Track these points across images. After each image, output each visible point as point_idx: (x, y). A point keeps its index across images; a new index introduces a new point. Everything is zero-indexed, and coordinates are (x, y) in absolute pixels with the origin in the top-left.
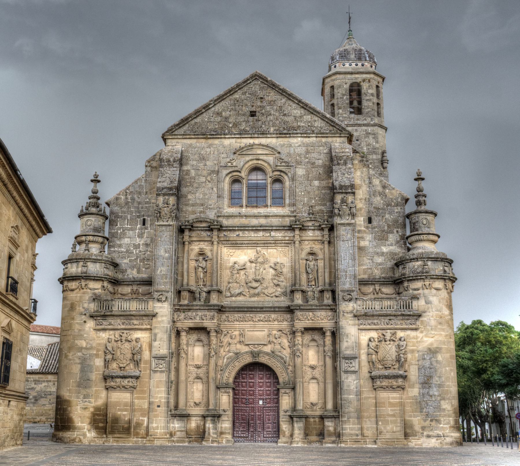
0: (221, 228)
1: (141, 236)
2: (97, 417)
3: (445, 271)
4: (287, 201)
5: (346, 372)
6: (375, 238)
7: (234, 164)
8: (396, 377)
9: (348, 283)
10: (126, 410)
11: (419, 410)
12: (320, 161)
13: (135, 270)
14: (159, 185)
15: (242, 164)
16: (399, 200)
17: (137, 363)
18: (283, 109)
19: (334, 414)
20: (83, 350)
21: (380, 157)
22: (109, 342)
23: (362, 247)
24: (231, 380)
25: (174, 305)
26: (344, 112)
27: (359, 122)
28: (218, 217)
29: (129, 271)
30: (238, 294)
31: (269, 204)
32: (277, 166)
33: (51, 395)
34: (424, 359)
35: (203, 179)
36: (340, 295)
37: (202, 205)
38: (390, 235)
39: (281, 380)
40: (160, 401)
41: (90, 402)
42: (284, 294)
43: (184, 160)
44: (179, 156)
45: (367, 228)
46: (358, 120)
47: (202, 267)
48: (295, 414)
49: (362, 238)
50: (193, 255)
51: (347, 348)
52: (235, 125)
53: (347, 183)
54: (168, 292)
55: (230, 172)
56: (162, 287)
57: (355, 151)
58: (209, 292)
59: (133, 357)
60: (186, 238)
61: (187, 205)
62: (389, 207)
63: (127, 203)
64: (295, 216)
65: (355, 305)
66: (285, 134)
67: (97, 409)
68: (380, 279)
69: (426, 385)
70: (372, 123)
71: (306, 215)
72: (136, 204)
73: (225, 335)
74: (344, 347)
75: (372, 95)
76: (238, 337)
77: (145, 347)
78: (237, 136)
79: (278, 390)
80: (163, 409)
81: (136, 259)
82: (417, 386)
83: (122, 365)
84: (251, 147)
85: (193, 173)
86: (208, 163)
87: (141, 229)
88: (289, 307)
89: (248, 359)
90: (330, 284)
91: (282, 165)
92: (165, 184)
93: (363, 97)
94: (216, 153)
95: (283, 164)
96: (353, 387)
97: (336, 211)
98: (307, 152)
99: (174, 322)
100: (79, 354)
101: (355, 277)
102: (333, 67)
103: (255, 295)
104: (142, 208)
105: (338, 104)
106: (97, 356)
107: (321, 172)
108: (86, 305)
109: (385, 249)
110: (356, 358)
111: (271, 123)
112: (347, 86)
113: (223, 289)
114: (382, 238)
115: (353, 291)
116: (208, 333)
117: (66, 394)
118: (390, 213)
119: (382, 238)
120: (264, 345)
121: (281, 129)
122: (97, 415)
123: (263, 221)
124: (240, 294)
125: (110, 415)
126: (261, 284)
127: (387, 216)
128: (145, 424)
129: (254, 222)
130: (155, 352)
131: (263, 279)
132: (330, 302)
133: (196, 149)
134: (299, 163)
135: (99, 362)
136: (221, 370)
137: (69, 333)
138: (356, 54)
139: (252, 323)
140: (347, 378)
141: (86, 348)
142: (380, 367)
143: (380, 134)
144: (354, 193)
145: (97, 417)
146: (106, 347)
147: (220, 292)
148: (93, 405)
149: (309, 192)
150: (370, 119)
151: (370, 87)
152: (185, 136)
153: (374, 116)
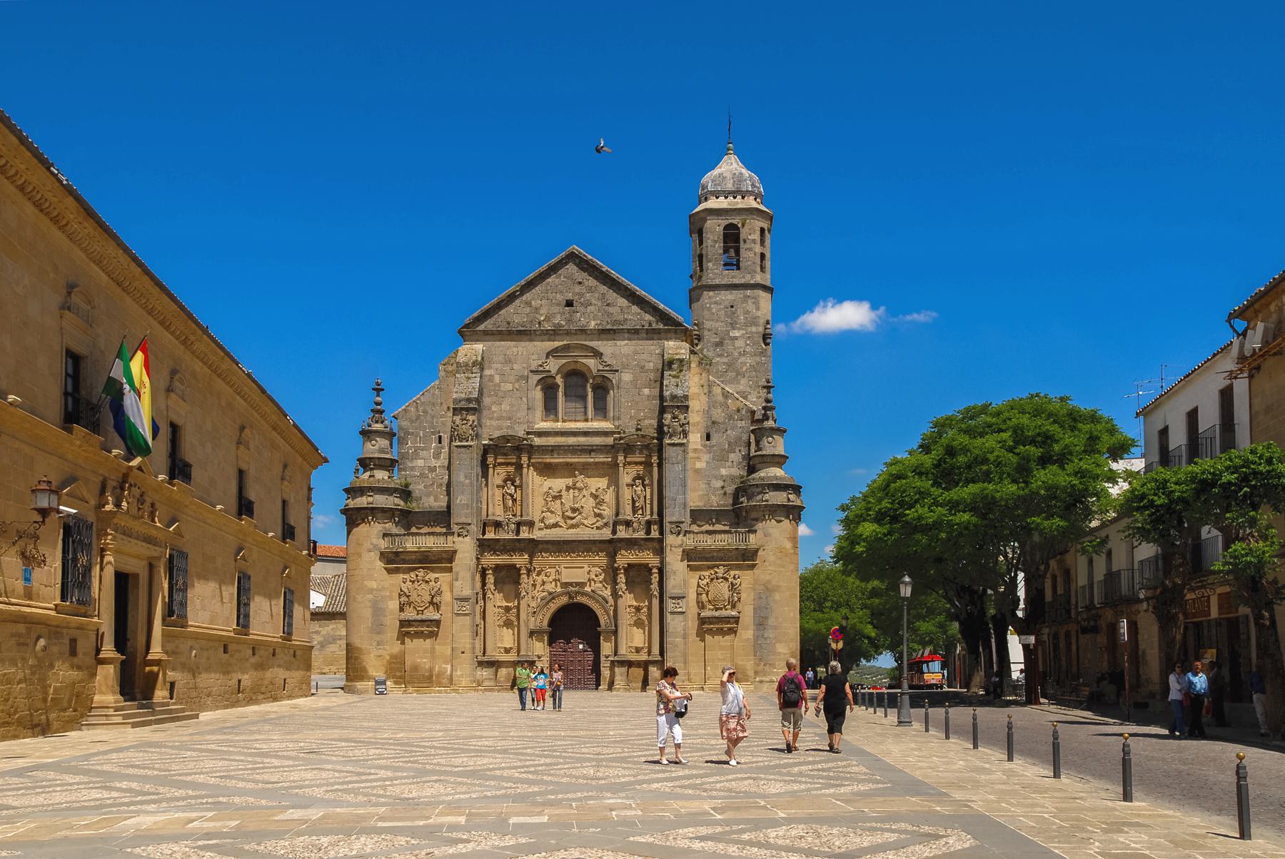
0: (531, 450)
1: (437, 456)
2: (393, 665)
3: (789, 499)
4: (612, 415)
5: (673, 613)
6: (714, 459)
7: (547, 368)
8: (727, 619)
9: (677, 513)
10: (426, 658)
11: (752, 653)
12: (651, 364)
13: (432, 497)
14: (455, 396)
15: (557, 367)
16: (744, 413)
17: (437, 607)
18: (607, 297)
19: (659, 658)
20: (374, 592)
21: (761, 329)
22: (404, 583)
23: (698, 469)
24: (546, 623)
25: (478, 540)
26: (715, 267)
27: (736, 281)
28: (528, 433)
29: (424, 499)
30: (553, 524)
31: (590, 417)
32: (598, 371)
33: (340, 639)
34: (760, 598)
35: (509, 387)
36: (667, 527)
37: (510, 419)
38: (732, 456)
39: (602, 622)
40: (465, 647)
41: (384, 649)
42: (606, 524)
43: (486, 365)
44: (480, 359)
45: (705, 446)
46: (733, 277)
47: (510, 495)
48: (616, 658)
49: (698, 458)
50: (499, 481)
51: (674, 587)
52: (548, 319)
53: (679, 392)
54: (470, 524)
55: (543, 378)
56: (463, 520)
57: (692, 352)
58: (519, 524)
59: (432, 598)
60: (490, 460)
61: (491, 419)
62: (731, 422)
63: (418, 417)
64: (619, 433)
65: (684, 538)
66: (609, 330)
67: (393, 657)
68: (718, 506)
69: (761, 627)
70: (752, 282)
71: (633, 431)
72: (429, 418)
73: (538, 574)
74: (671, 585)
75: (754, 241)
76: (553, 573)
77: (445, 588)
78: (551, 332)
79: (599, 634)
80: (468, 655)
81: (433, 484)
82: (752, 627)
83: (420, 609)
84: (566, 348)
85: (497, 379)
86: (515, 366)
87: (436, 448)
88: (611, 541)
89: (564, 600)
90: (661, 514)
91: (605, 368)
92: (463, 396)
93: (742, 244)
94: (525, 353)
95: (608, 368)
96: (680, 630)
97: (665, 428)
98: (636, 353)
99: (478, 559)
100: (370, 596)
101: (685, 505)
102: (703, 198)
103: (573, 526)
104: (437, 422)
105: (707, 255)
106: (391, 599)
107: (652, 378)
108: (375, 541)
109: (724, 472)
110: (684, 597)
111: (592, 315)
112: (720, 230)
113: (536, 519)
114: (721, 458)
115: (683, 522)
116: (519, 569)
117: (357, 642)
118: (732, 429)
119: (721, 458)
120: (582, 585)
121: (604, 323)
122: (394, 663)
123: (582, 440)
124: (556, 525)
125: (408, 663)
126: (580, 513)
127: (729, 432)
128: (449, 672)
129: (572, 440)
130: (457, 593)
131: (582, 507)
132: (657, 533)
133: (501, 349)
134: (625, 366)
135: (393, 605)
136: (535, 612)
137: (357, 572)
138: (734, 182)
139: (569, 558)
140: (673, 620)
141: (376, 590)
142: (712, 607)
143: (763, 298)
144: (687, 407)
145: (393, 665)
146: (401, 590)
147: (531, 524)
148: (389, 652)
149: (637, 403)
150: (749, 276)
151: (752, 231)
152: (488, 335)
153: (755, 272)
